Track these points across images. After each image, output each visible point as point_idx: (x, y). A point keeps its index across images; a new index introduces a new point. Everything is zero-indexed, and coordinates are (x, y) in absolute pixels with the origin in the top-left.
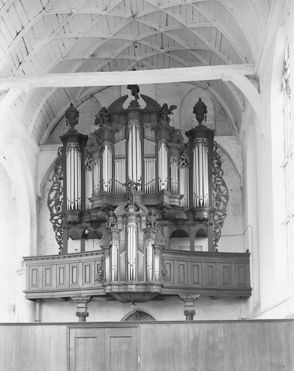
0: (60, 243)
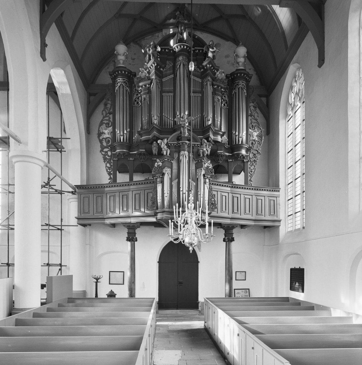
0: (109, 174)
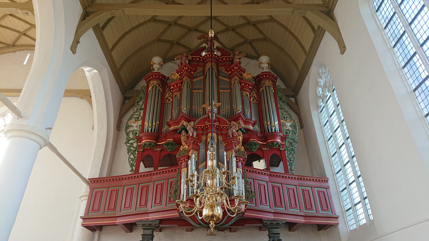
0: (132, 165)
